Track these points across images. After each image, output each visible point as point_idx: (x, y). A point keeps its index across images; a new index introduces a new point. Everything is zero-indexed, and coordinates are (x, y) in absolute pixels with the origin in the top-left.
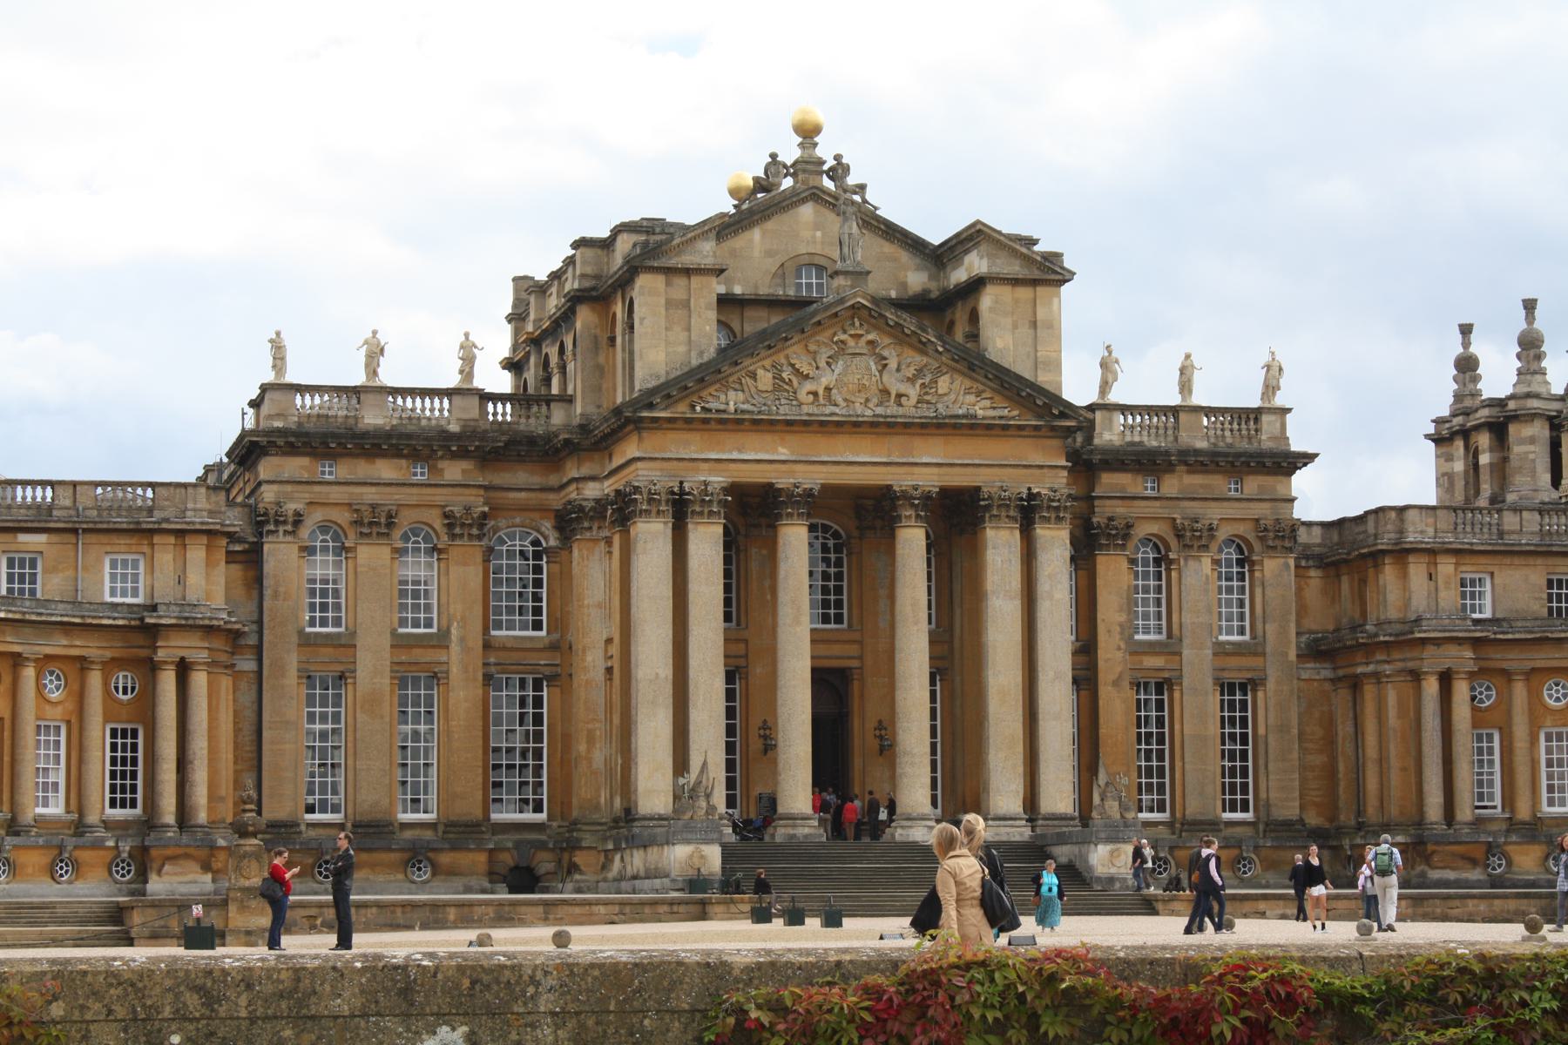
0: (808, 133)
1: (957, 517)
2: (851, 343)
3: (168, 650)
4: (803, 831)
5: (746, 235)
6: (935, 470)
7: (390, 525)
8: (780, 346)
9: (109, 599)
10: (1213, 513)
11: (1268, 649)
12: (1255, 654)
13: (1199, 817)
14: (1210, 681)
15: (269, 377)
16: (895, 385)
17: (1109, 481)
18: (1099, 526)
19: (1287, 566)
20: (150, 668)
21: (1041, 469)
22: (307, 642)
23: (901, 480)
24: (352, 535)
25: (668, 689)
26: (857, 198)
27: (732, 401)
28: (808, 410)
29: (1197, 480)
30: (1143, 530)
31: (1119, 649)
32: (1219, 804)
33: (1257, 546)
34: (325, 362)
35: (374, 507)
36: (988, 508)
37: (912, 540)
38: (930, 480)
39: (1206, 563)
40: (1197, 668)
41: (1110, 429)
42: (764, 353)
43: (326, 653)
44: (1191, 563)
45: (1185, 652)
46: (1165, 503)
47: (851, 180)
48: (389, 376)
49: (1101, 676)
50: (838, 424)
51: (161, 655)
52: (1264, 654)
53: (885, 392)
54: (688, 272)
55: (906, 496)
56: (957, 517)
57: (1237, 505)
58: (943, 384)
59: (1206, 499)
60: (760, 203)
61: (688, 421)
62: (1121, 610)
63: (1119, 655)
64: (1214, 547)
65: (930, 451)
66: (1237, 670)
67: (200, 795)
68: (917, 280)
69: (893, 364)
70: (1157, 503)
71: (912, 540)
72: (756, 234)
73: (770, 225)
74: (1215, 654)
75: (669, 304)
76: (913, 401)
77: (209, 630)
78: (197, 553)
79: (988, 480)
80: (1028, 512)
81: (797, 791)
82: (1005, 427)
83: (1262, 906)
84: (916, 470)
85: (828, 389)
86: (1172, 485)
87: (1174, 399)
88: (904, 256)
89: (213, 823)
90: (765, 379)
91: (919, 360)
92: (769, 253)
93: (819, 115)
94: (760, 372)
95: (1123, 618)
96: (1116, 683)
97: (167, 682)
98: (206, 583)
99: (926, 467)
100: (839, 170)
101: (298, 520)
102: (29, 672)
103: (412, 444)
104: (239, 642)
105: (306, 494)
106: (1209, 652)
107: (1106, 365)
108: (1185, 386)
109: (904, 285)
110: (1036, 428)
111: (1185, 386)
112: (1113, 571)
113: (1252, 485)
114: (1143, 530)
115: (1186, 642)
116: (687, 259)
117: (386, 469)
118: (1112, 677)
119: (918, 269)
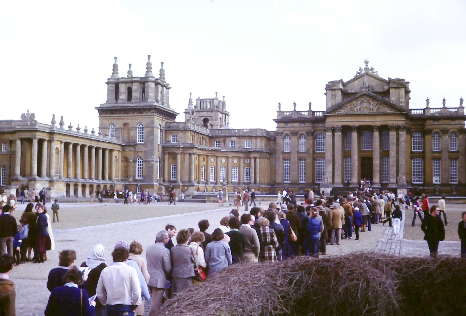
0: (367, 63)
3: (252, 155)
4: (354, 186)
5: (354, 82)
7: (297, 134)
9: (246, 147)
14: (447, 158)
15: (278, 110)
16: (372, 107)
20: (250, 158)
21: (400, 121)
22: (283, 153)
24: (291, 135)
25: (332, 161)
26: (375, 74)
28: (356, 113)
30: (434, 131)
32: (450, 181)
34: (288, 108)
35: (294, 131)
37: (376, 134)
38: (379, 124)
39: (447, 137)
43: (287, 155)
44: (444, 136)
47: (375, 71)
48: (297, 110)
49: (426, 157)
51: (251, 156)
53: (370, 108)
54: (335, 90)
56: (384, 130)
60: (358, 77)
64: (449, 134)
67: (258, 179)
68: (386, 88)
75: (332, 95)
77: (259, 152)
78: (259, 140)
79: (389, 123)
85: (360, 108)
87: (442, 106)
88: (384, 84)
89: (261, 183)
93: (368, 60)
97: (253, 160)
98: (260, 145)
99: (378, 121)
100: (372, 69)
102: (230, 159)
103: (301, 120)
104: (271, 153)
105: (284, 129)
107: (427, 100)
108: (444, 104)
109: (383, 89)
111: (444, 104)
112: (428, 137)
113: (457, 122)
114: (434, 131)
116: (335, 87)
117: (296, 125)
119: (386, 85)
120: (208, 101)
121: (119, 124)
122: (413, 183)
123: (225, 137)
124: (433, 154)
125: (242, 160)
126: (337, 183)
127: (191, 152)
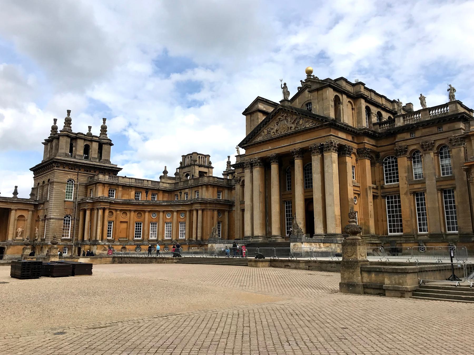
1: (306, 154)
2: (281, 117)
6: (300, 144)
8: (268, 123)
10: (433, 138)
11: (456, 178)
12: (452, 180)
13: (435, 233)
14: (436, 190)
15: (237, 154)
17: (400, 137)
18: (396, 150)
19: (460, 150)
23: (291, 149)
27: (259, 139)
29: (427, 130)
31: (406, 184)
33: (450, 146)
36: (311, 151)
38: (298, 147)
39: (432, 154)
40: (431, 186)
41: (400, 122)
42: (265, 126)
44: (427, 155)
45: (427, 182)
46: (416, 139)
50: (278, 138)
52: (454, 179)
55: (293, 152)
56: (306, 154)
57: (441, 134)
58: (301, 122)
59: (430, 135)
61: (252, 145)
62: (405, 173)
63: (406, 186)
65: (299, 139)
66: (446, 185)
69: (289, 120)
70: (414, 140)
71: (298, 163)
72: (297, 100)
73: (300, 97)
74: (436, 181)
76: (293, 128)
77: (200, 203)
80: (322, 149)
81: (275, 231)
82: (314, 128)
83: (290, 264)
84: (296, 145)
85: (277, 131)
86: (418, 134)
90: (265, 131)
91: (296, 117)
92: (300, 103)
94: (265, 130)
95: (406, 175)
96: (406, 194)
97: (195, 213)
99: (298, 143)
101: (240, 181)
102: (175, 213)
106: (435, 181)
110: (321, 126)
111: (423, 103)
115: (427, 179)
118: (404, 193)
120: (189, 156)
121: (41, 182)
122: (389, 234)
123: (181, 190)
124: (412, 187)
125: (188, 213)
126: (258, 237)
127: (98, 207)
